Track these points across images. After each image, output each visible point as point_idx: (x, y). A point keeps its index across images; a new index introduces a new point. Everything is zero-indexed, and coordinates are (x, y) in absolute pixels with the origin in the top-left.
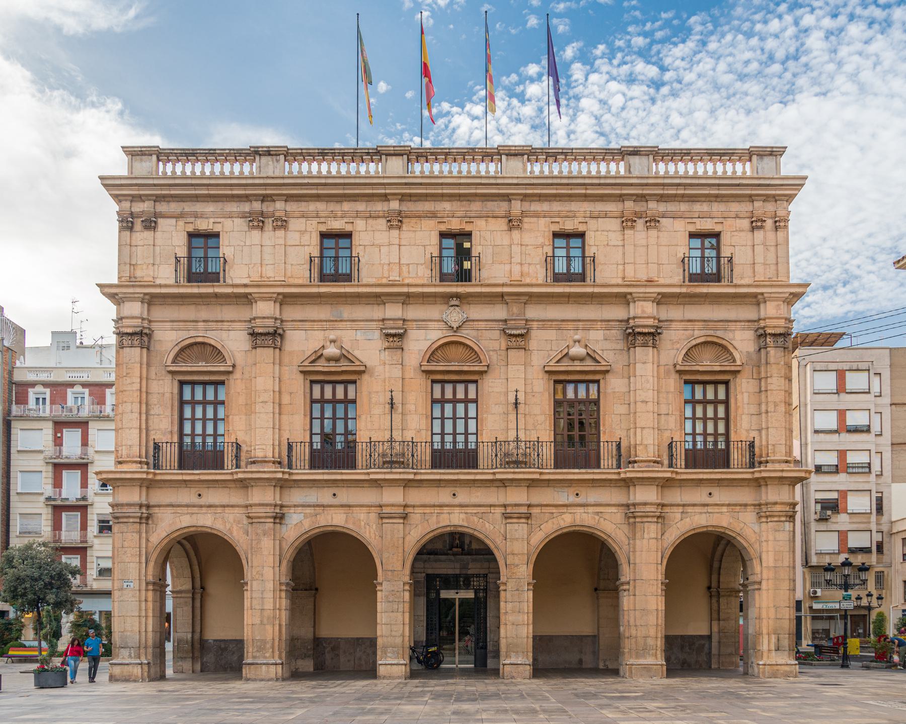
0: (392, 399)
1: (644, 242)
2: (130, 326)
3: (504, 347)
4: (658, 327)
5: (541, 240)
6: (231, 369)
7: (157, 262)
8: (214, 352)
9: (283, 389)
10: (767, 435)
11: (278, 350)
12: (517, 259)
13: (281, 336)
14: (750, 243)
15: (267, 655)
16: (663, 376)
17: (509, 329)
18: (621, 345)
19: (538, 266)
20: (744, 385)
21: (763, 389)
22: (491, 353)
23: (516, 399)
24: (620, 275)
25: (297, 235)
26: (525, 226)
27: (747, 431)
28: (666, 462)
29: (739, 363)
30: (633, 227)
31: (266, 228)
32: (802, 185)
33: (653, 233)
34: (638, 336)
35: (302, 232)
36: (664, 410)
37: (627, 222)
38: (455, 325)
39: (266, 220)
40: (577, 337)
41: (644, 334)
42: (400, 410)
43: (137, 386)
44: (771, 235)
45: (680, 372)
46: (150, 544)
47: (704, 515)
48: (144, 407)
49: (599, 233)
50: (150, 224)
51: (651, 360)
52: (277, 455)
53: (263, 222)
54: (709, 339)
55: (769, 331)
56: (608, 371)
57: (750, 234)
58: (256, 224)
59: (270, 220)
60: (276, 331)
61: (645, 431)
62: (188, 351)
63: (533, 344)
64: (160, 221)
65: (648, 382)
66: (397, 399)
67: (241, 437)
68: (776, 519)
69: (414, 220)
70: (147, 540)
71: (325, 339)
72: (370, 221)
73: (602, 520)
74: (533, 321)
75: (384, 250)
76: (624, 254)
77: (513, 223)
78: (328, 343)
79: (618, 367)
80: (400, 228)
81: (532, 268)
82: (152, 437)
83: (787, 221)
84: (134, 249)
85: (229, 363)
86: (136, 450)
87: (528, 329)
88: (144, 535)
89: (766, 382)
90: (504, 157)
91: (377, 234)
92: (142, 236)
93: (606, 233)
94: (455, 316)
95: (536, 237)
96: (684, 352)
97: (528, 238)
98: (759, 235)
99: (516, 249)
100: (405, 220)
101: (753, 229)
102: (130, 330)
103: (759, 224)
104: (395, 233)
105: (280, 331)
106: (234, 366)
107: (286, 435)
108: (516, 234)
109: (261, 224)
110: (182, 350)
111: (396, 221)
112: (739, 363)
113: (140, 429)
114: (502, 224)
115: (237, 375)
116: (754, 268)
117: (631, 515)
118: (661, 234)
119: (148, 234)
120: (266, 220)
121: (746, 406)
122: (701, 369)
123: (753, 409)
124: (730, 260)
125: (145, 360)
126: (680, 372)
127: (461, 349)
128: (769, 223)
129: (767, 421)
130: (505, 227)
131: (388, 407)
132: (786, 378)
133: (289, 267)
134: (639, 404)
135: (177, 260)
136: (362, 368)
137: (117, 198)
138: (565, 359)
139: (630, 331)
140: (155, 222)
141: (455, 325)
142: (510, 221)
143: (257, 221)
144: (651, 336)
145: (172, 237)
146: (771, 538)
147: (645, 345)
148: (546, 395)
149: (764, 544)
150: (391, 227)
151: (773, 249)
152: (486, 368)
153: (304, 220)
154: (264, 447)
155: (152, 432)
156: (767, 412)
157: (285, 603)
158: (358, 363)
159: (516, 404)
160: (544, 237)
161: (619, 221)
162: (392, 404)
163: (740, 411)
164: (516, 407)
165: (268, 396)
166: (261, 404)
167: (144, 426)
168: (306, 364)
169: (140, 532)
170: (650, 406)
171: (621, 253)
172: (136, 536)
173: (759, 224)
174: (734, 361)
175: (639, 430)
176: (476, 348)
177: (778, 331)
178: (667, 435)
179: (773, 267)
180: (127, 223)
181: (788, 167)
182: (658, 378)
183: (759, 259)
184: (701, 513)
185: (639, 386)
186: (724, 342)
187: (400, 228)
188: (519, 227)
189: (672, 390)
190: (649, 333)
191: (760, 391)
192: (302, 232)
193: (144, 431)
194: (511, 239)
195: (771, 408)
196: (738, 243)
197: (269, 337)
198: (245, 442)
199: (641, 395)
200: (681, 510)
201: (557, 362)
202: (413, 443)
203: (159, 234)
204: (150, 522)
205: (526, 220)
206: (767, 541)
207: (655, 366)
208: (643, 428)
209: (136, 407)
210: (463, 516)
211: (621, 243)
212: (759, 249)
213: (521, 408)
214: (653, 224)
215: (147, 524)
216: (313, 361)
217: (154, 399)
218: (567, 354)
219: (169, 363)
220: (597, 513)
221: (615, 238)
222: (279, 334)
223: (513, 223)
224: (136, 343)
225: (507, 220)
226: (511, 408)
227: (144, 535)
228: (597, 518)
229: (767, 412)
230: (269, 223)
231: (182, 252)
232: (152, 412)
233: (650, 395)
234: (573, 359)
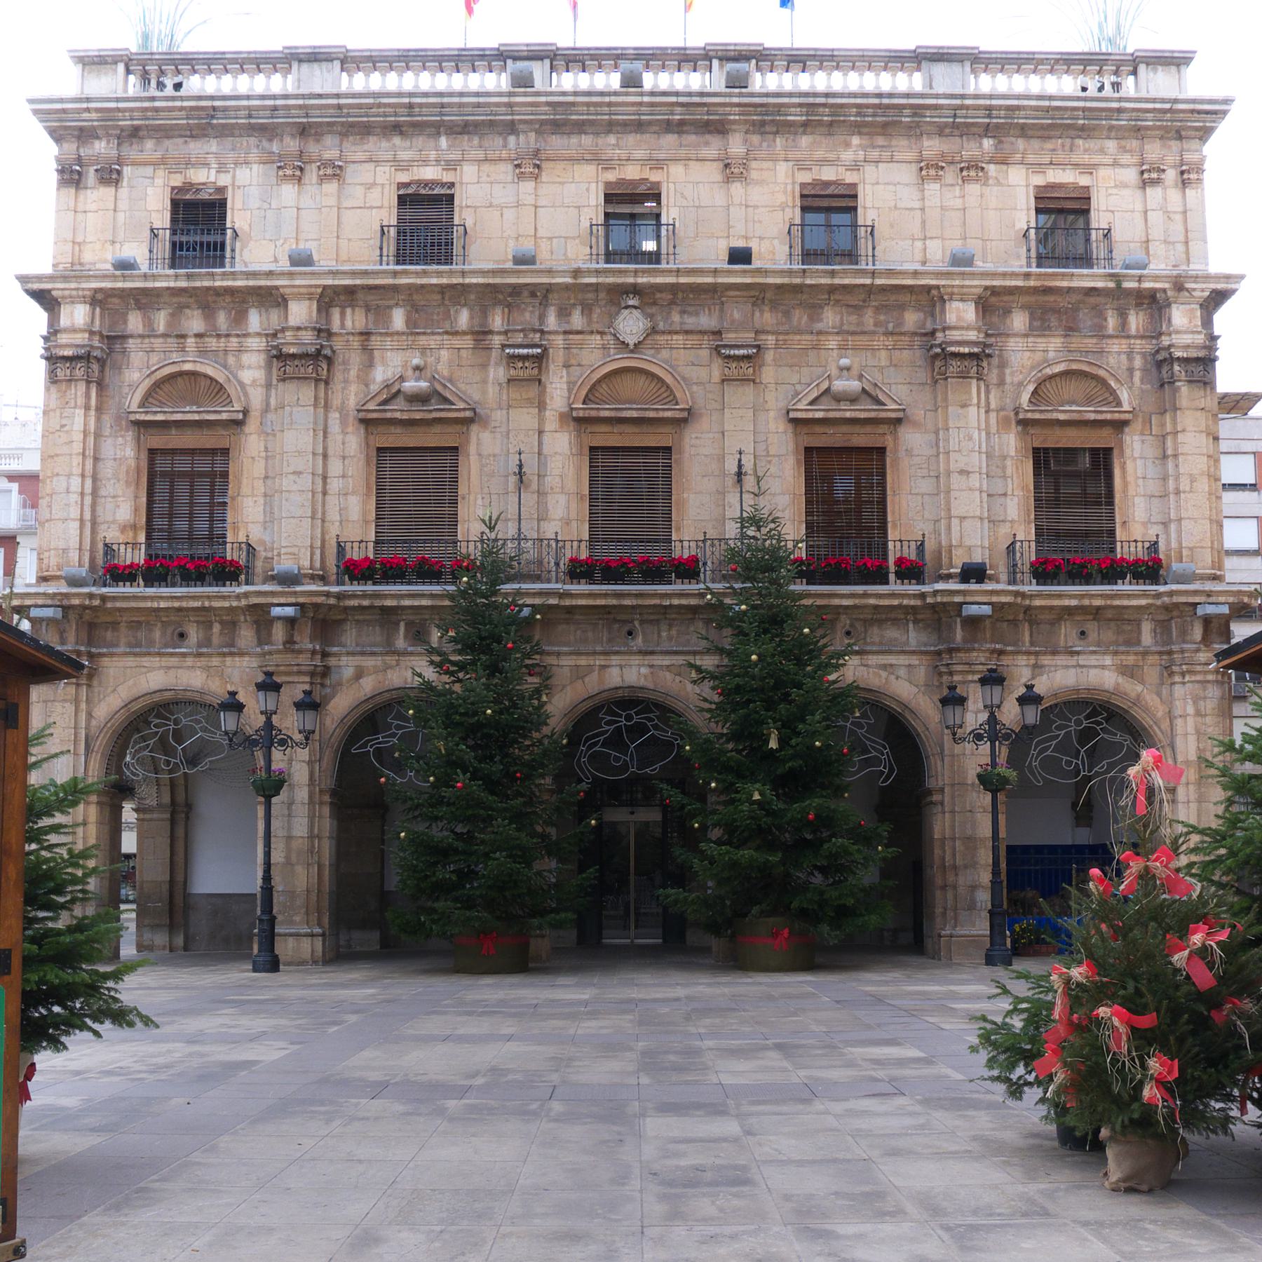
0: (521, 466)
1: (958, 203)
2: (69, 343)
3: (716, 375)
4: (985, 345)
5: (781, 198)
6: (241, 416)
7: (121, 236)
8: (217, 390)
9: (330, 452)
10: (1179, 532)
11: (322, 386)
12: (739, 228)
13: (330, 361)
14: (1139, 207)
15: (297, 918)
16: (994, 429)
17: (725, 346)
18: (923, 375)
19: (776, 242)
20: (1137, 446)
21: (1170, 452)
22: (695, 388)
23: (740, 466)
24: (919, 257)
25: (359, 191)
26: (754, 175)
27: (1144, 524)
28: (1004, 577)
29: (1126, 407)
30: (937, 178)
31: (306, 179)
32: (1225, 113)
33: (973, 189)
34: (948, 363)
35: (370, 186)
36: (998, 487)
37: (929, 169)
38: (631, 341)
39: (308, 167)
40: (844, 362)
41: (962, 356)
42: (534, 486)
43: (78, 447)
44: (1174, 195)
45: (1024, 423)
46: (94, 723)
47: (1073, 671)
48: (89, 482)
49: (881, 187)
50: (110, 176)
51: (975, 401)
52: (318, 565)
53: (301, 169)
54: (1074, 366)
55: (1178, 354)
56: (899, 421)
57: (1139, 193)
58: (289, 172)
59: (314, 166)
60: (319, 352)
61: (966, 524)
62: (167, 387)
63: (768, 374)
64: (127, 171)
65: (970, 438)
66: (530, 469)
67: (255, 533)
68: (1199, 678)
69: (561, 165)
70: (90, 715)
71: (405, 366)
72: (486, 167)
73: (893, 677)
74: (768, 332)
75: (509, 214)
76: (924, 222)
77: (732, 171)
78: (410, 372)
79: (918, 413)
80: (537, 178)
81: (766, 245)
82: (100, 536)
83: (1200, 170)
84: (80, 216)
85: (237, 407)
86: (74, 556)
87: (758, 347)
88: (83, 706)
89: (1175, 439)
90: (715, 63)
91: (496, 187)
92: (96, 196)
93: (891, 188)
94: (631, 325)
95: (773, 193)
96: (1031, 388)
97: (757, 195)
98: (1154, 193)
99: (737, 213)
100: (544, 165)
101: (1144, 184)
102: (68, 352)
103: (1154, 175)
104: (528, 186)
105: (327, 352)
106: (245, 412)
107: (334, 530)
108: (737, 188)
109: (298, 173)
110: (158, 385)
111: (531, 166)
112: (1126, 407)
113: (82, 520)
114: (712, 172)
115: (251, 426)
116: (1147, 248)
117: (943, 669)
118: (987, 190)
119: (108, 192)
120: (308, 167)
121: (1140, 482)
122: (1062, 417)
123: (1153, 487)
124: (1107, 234)
125: (93, 402)
126: (1024, 423)
127: (642, 381)
128: (1171, 175)
129: (1178, 507)
130: (719, 178)
131: (513, 480)
132: (1208, 434)
133: (343, 243)
134: (955, 478)
135: (154, 233)
136: (468, 414)
137: (57, 135)
138: (824, 399)
139: (938, 350)
140: (119, 172)
141: (631, 341)
142: (727, 166)
143: (294, 170)
144: (978, 360)
145: (147, 198)
146: (1190, 710)
147: (964, 376)
148: (791, 461)
149: (1179, 722)
150: (521, 177)
151: (1178, 217)
152: (685, 414)
153: (373, 165)
154: (295, 550)
155: (103, 527)
156: (1178, 492)
157: (327, 824)
158: (462, 405)
159: (740, 474)
160: (785, 192)
161: (914, 167)
162: (520, 474)
163: (1131, 492)
164: (740, 481)
165: (305, 463)
166: (292, 477)
167: (88, 516)
168: (371, 406)
169: (77, 701)
170: (975, 481)
171: (918, 222)
172: (70, 708)
173: (1154, 175)
174: (1119, 404)
175: (955, 522)
176: (669, 379)
177: (1193, 354)
178: (1004, 530)
179: (1180, 248)
180: (71, 176)
181: (1196, 84)
182: (988, 434)
183: (1156, 233)
184: (1067, 667)
185: (953, 445)
186: (1101, 373)
187: (537, 178)
188: (742, 178)
189: (1013, 453)
190: (971, 355)
191: (1165, 457)
192: (370, 186)
193: (88, 525)
194: (729, 196)
195: (1184, 484)
196: (1118, 204)
197: (306, 363)
198: (262, 542)
199: (958, 461)
200: (1033, 662)
201: (811, 403)
202: (557, 541)
203: (124, 192)
204: (95, 683)
205: (754, 164)
206: (1184, 716)
207: (983, 411)
208: (962, 519)
209: (76, 482)
210: (644, 670)
211: (917, 205)
212: (1155, 218)
213: (749, 482)
214: (972, 173)
215: (89, 686)
216: (385, 402)
217: (107, 469)
218: (827, 391)
219: (134, 407)
220: (884, 667)
221: (909, 197)
222: (326, 357)
223: (732, 171)
224: (79, 373)
225: (721, 165)
226: (730, 481)
227: (83, 706)
228: (884, 674)
229: (1178, 492)
230: (312, 174)
231: (163, 219)
232: (103, 492)
233: (976, 461)
234: (838, 398)
